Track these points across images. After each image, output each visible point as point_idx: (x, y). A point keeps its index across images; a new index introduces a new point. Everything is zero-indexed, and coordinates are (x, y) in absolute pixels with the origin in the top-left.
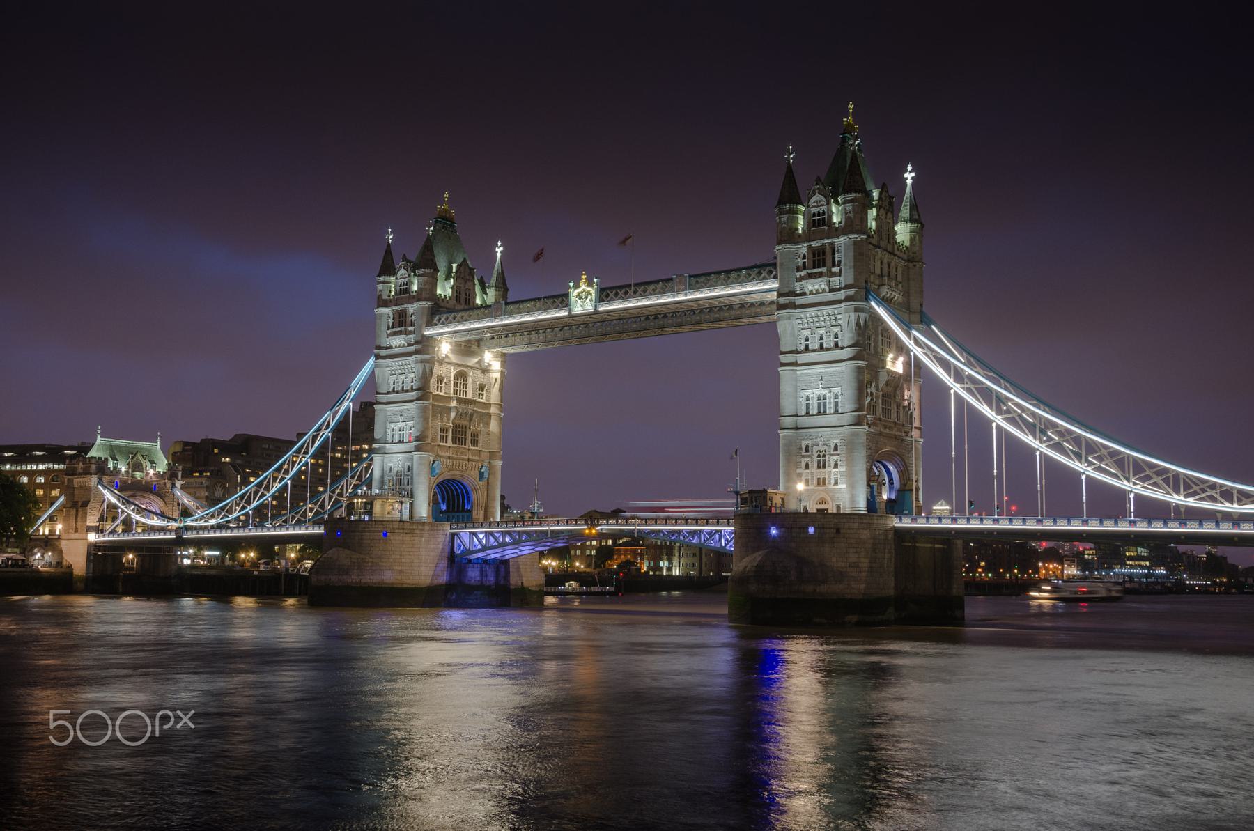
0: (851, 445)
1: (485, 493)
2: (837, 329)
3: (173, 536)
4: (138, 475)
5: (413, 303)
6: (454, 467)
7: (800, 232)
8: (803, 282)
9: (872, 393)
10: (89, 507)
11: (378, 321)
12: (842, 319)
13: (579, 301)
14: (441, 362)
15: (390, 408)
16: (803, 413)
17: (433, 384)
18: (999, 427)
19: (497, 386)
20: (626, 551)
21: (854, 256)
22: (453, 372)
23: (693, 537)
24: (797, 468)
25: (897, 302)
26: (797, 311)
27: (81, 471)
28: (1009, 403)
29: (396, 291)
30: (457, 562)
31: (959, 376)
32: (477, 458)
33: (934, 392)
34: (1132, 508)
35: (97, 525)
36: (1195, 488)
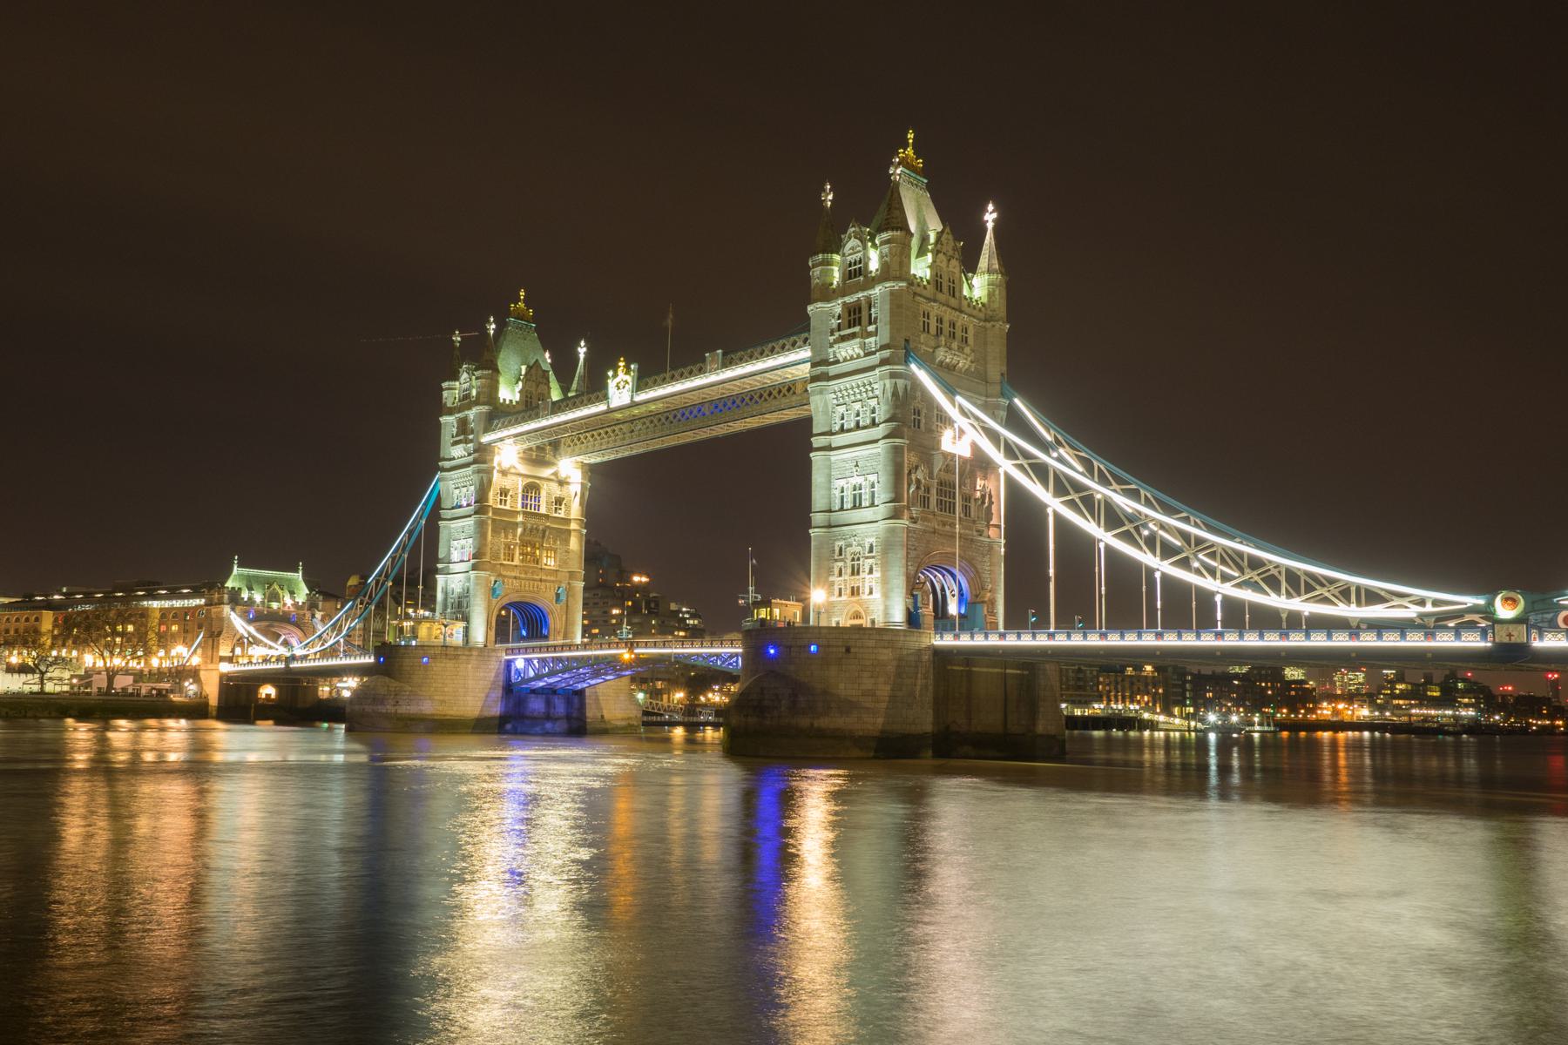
0: (887, 546)
1: (564, 616)
2: (873, 402)
3: (281, 666)
4: (275, 605)
5: (470, 409)
6: (523, 588)
8: (836, 346)
9: (918, 481)
10: (222, 637)
13: (617, 392)
14: (504, 473)
16: (837, 509)
18: (1058, 518)
21: (891, 309)
22: (521, 483)
25: (963, 370)
26: (830, 383)
27: (216, 601)
30: (512, 690)
32: (552, 578)
35: (231, 654)
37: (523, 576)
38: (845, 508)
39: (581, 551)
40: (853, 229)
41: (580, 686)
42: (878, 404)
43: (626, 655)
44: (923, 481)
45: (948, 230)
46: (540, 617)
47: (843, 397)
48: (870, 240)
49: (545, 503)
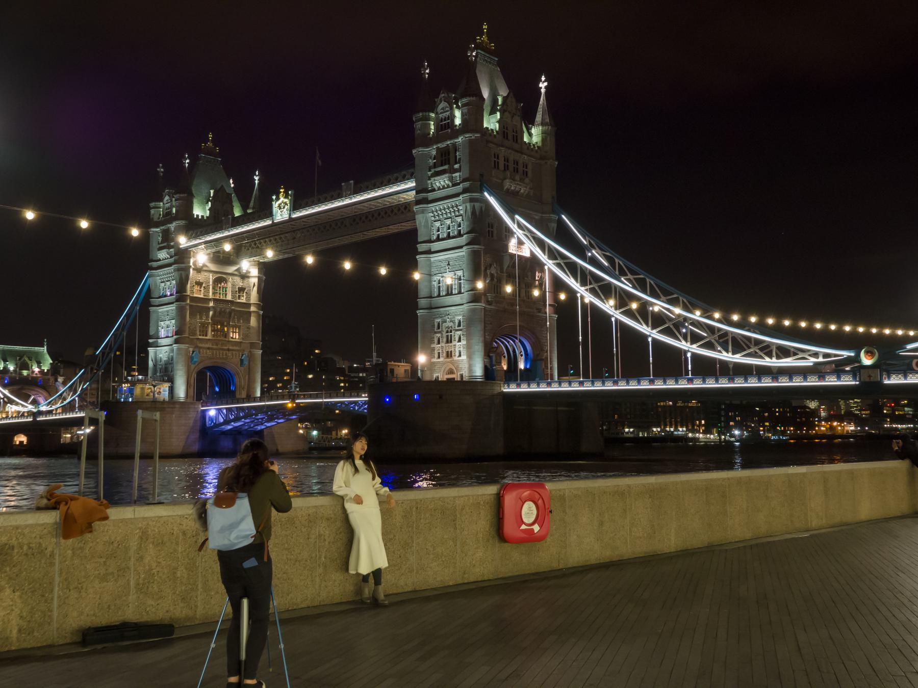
0: (470, 321)
2: (459, 219)
3: (30, 419)
4: (25, 373)
5: (171, 223)
8: (432, 179)
9: (491, 274)
13: (279, 211)
14: (199, 270)
16: (436, 295)
19: (255, 289)
22: (211, 277)
24: (431, 343)
26: (429, 205)
29: (163, 214)
32: (237, 348)
34: (690, 366)
37: (215, 347)
38: (441, 294)
39: (259, 327)
40: (443, 95)
41: (259, 428)
42: (463, 221)
44: (496, 275)
45: (511, 94)
47: (438, 215)
49: (230, 292)
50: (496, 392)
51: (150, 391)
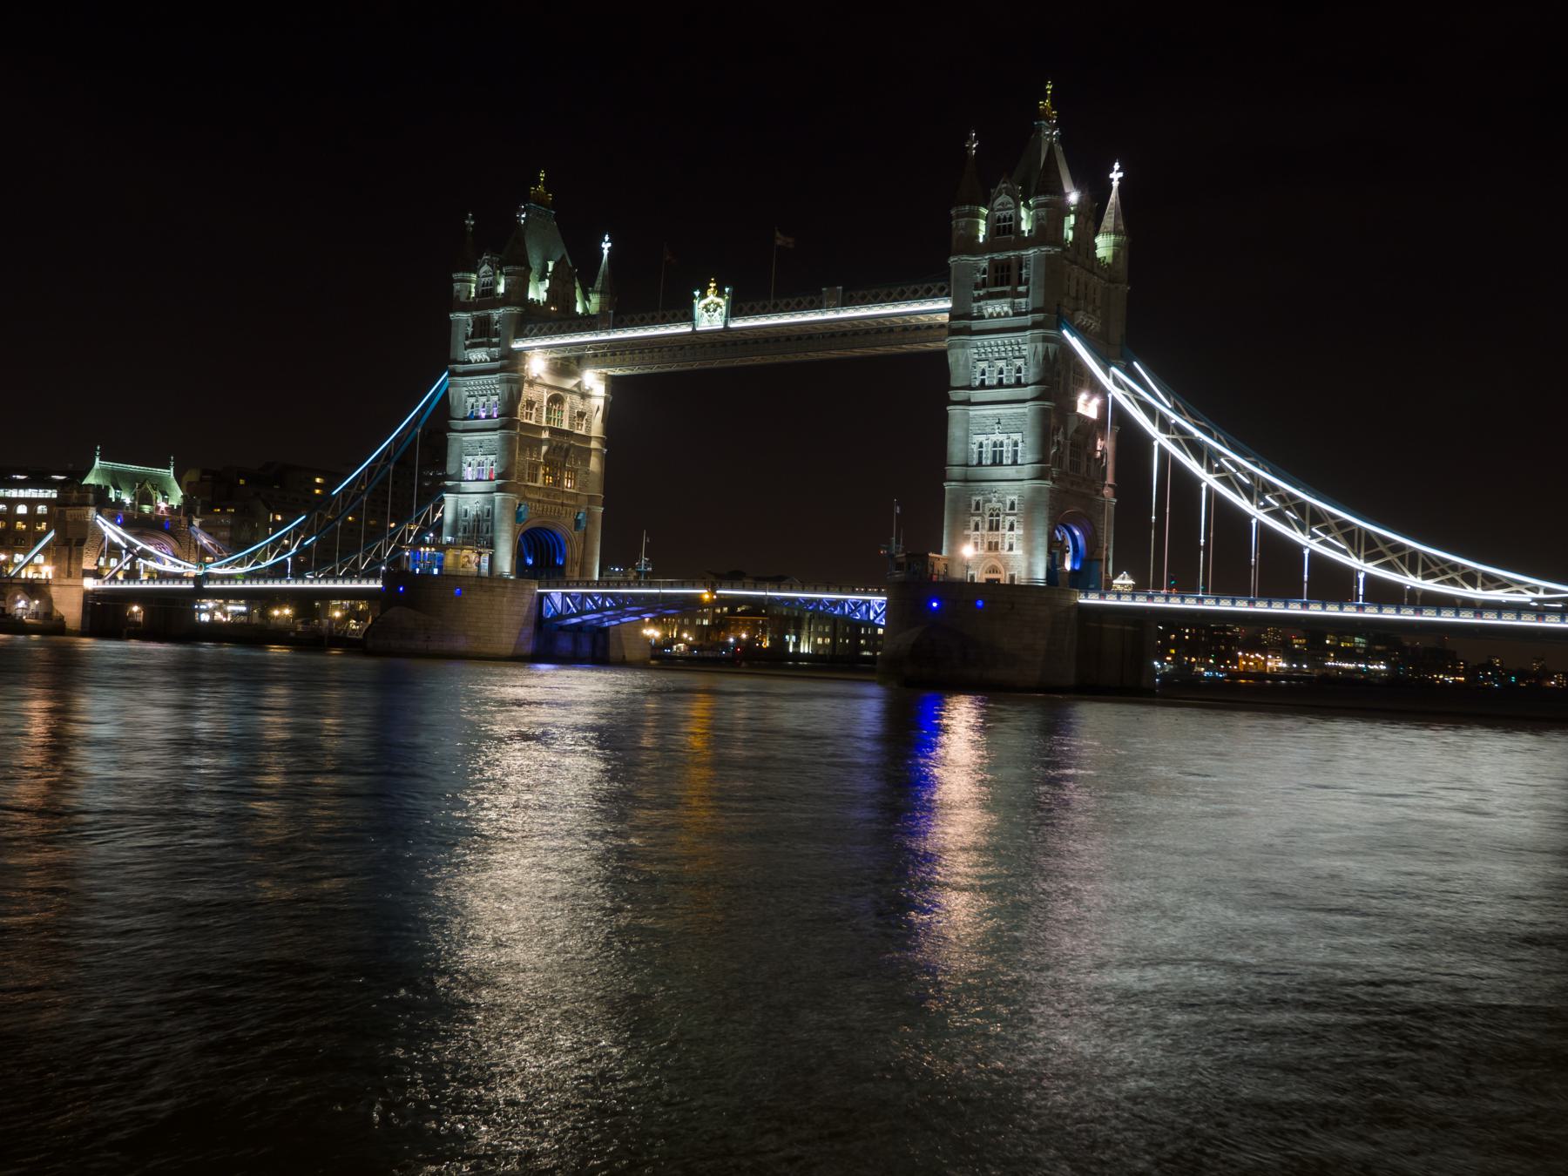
2: (1020, 362)
3: (191, 585)
4: (146, 509)
5: (498, 308)
7: (981, 240)
8: (982, 303)
11: (453, 329)
12: (1027, 349)
13: (706, 315)
14: (532, 383)
15: (467, 437)
16: (975, 462)
17: (521, 409)
19: (600, 415)
20: (746, 621)
22: (546, 395)
23: (836, 609)
27: (76, 501)
28: (1222, 460)
31: (1165, 426)
32: (572, 503)
33: (1132, 442)
36: (1435, 569)
38: (984, 463)
40: (1005, 185)
43: (706, 595)
46: (554, 543)
48: (1022, 199)
50: (1072, 603)
51: (466, 560)
